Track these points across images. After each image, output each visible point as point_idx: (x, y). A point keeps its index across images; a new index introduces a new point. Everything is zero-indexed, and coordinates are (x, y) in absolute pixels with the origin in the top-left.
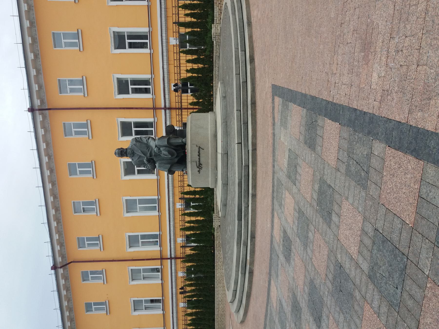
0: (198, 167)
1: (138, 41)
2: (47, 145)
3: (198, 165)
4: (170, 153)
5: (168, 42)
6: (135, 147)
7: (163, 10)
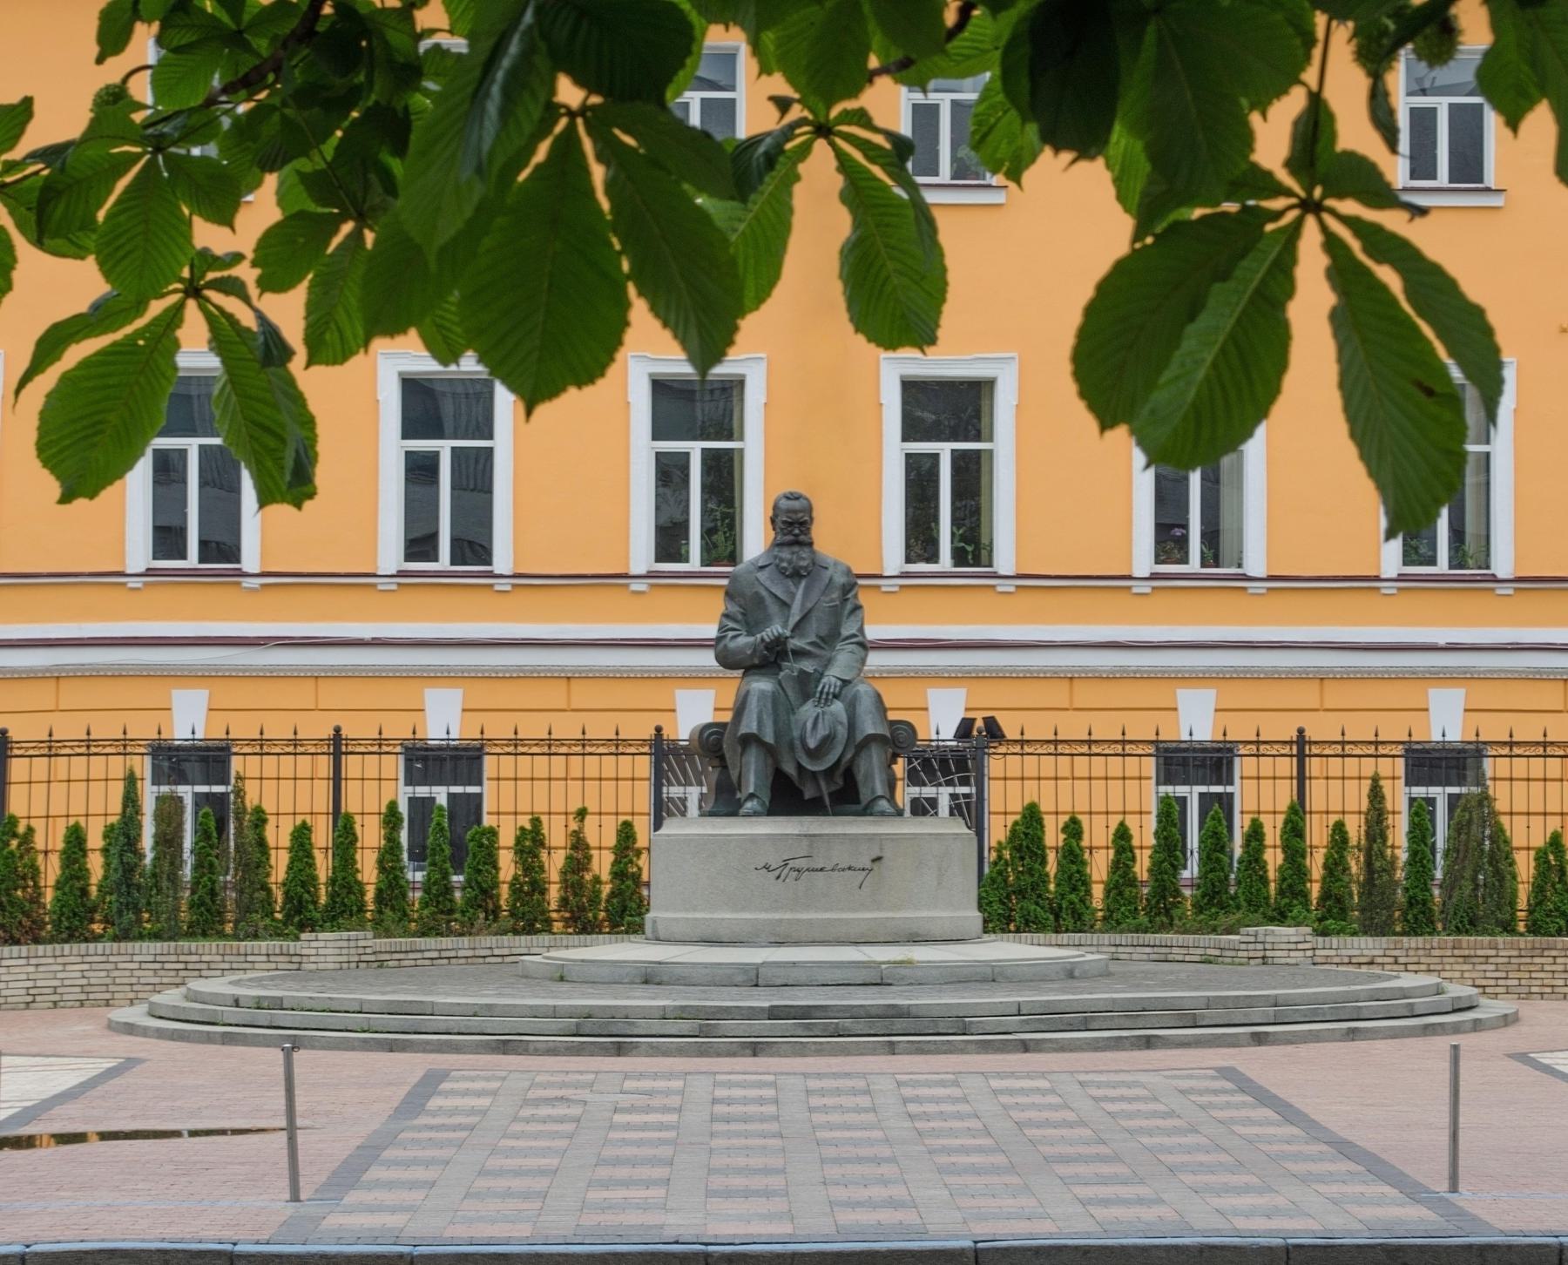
4: (828, 741)
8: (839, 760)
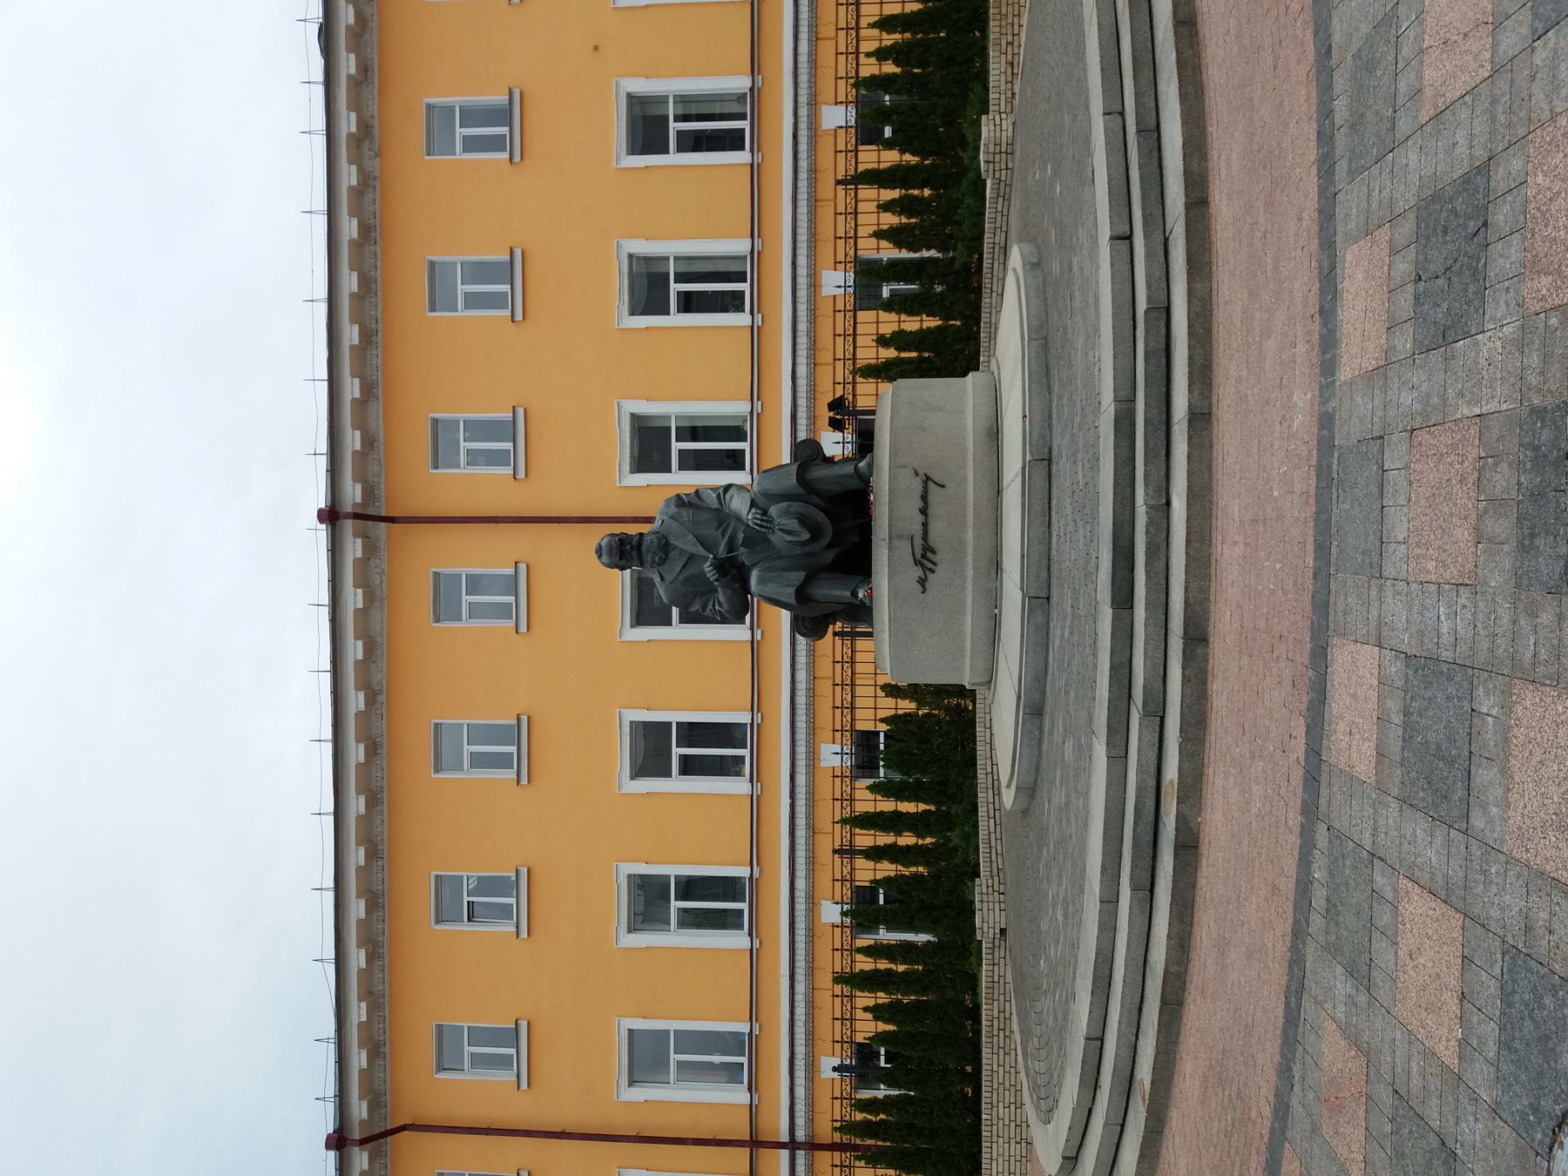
0: (916, 562)
1: (713, 288)
2: (370, 648)
3: (918, 552)
4: (803, 520)
5: (814, 285)
6: (674, 525)
7: (803, 176)
8: (823, 510)
